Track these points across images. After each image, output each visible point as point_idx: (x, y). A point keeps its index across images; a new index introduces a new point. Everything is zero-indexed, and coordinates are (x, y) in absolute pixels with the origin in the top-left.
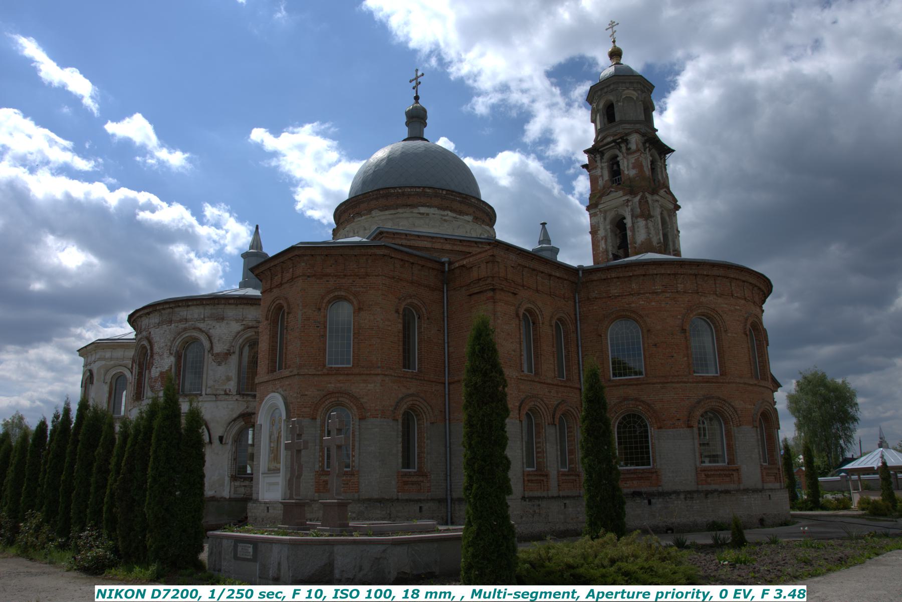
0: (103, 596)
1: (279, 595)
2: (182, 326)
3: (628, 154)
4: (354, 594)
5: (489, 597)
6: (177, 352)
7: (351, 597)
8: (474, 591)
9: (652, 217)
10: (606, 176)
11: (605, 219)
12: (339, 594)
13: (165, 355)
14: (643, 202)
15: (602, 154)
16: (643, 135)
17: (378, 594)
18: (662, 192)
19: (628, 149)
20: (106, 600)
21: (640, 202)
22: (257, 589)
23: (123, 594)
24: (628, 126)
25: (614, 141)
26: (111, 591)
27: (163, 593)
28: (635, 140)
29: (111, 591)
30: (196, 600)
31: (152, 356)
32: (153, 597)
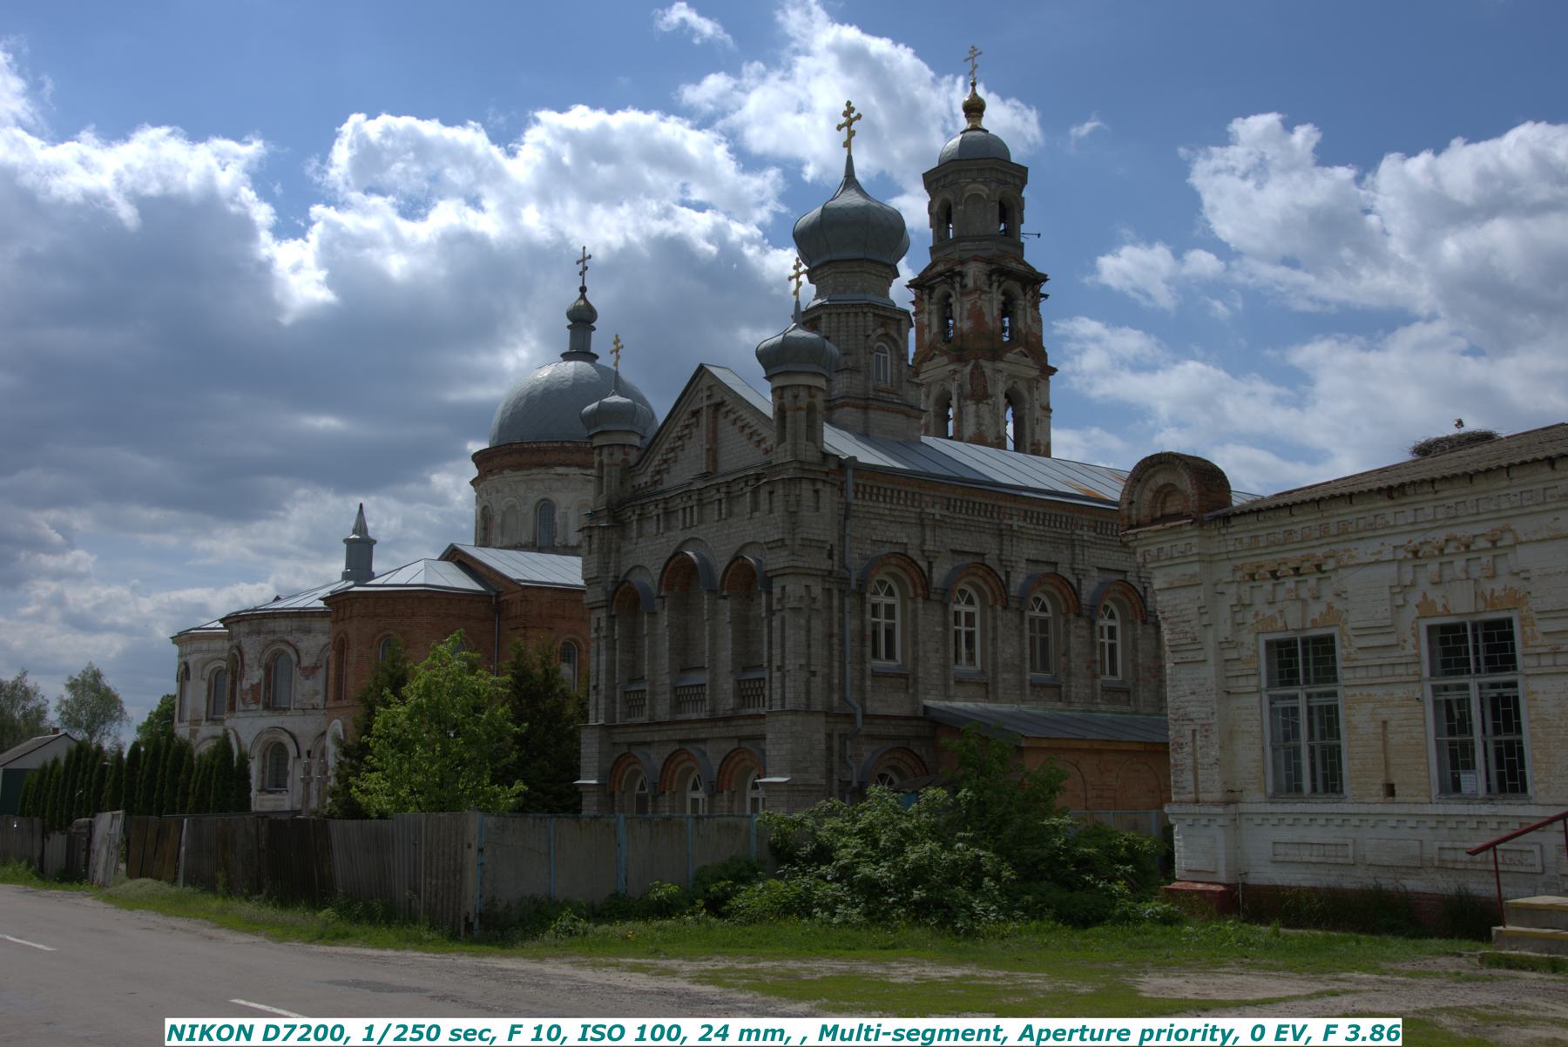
0: (180, 1037)
1: (485, 1035)
4: (616, 1033)
5: (850, 1039)
7: (610, 1038)
8: (824, 1027)
9: (987, 396)
12: (590, 1033)
14: (978, 373)
17: (657, 1034)
20: (184, 1043)
21: (972, 373)
22: (447, 1024)
23: (213, 1033)
26: (193, 1027)
27: (284, 1032)
29: (193, 1027)
30: (340, 1043)
32: (265, 1038)
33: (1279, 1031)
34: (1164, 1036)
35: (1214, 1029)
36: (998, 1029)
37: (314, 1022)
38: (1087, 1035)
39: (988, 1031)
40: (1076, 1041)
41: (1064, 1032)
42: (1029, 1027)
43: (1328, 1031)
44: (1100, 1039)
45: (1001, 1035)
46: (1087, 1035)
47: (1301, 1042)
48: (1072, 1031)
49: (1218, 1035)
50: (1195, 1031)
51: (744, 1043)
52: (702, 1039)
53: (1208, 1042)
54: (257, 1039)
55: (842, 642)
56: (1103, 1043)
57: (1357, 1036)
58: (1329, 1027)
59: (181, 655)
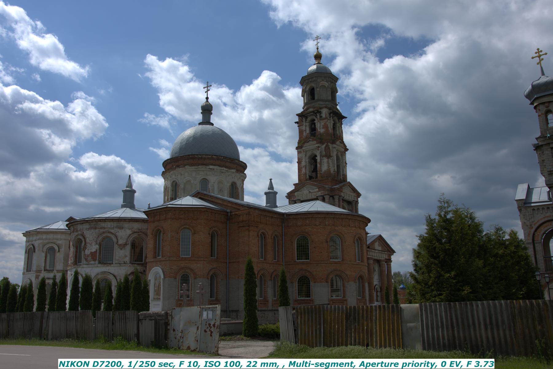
0: (63, 366)
1: (171, 365)
2: (102, 230)
3: (320, 120)
4: (217, 364)
5: (300, 366)
6: (100, 243)
7: (215, 366)
8: (291, 362)
9: (331, 157)
10: (308, 131)
11: (306, 156)
12: (208, 364)
13: (93, 244)
14: (327, 148)
15: (306, 118)
16: (330, 109)
17: (232, 364)
18: (338, 143)
19: (321, 117)
20: (65, 368)
21: (325, 148)
22: (158, 361)
23: (75, 364)
24: (321, 103)
25: (313, 112)
26: (68, 362)
27: (100, 364)
28: (325, 112)
29: (68, 362)
30: (120, 368)
31: (85, 244)
32: (94, 366)
33: (451, 364)
34: (411, 365)
35: (428, 363)
36: (352, 363)
37: (111, 360)
38: (383, 365)
39: (348, 363)
40: (379, 367)
41: (375, 364)
42: (363, 362)
43: (469, 363)
44: (388, 366)
45: (353, 365)
46: (383, 365)
47: (459, 367)
48: (378, 363)
49: (430, 365)
50: (421, 363)
51: (263, 367)
52: (248, 366)
53: (426, 367)
54: (91, 366)
56: (389, 367)
57: (479, 365)
58: (469, 362)
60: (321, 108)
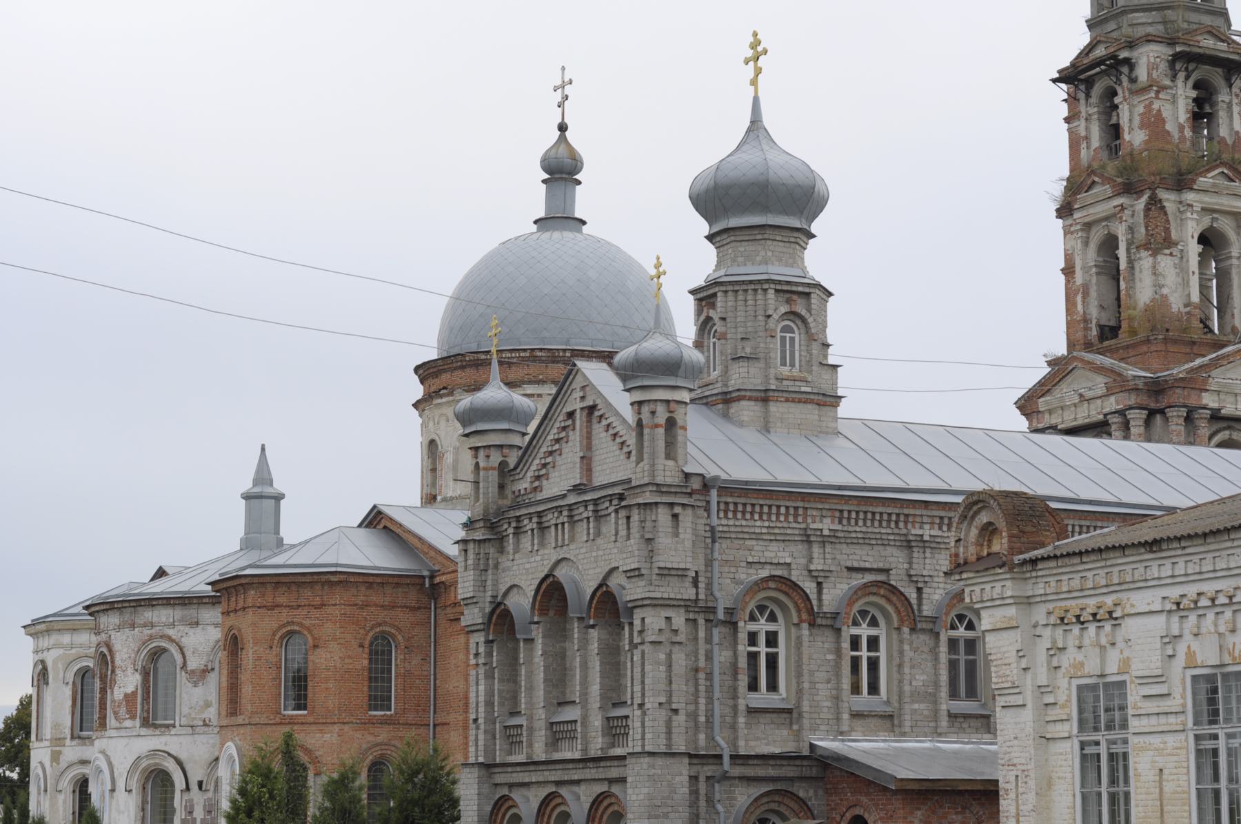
6: (143, 667)
9: (1168, 243)
11: (1086, 243)
21: (1147, 209)
31: (113, 671)
55: (710, 676)
59: (36, 652)
60: (1131, 45)
